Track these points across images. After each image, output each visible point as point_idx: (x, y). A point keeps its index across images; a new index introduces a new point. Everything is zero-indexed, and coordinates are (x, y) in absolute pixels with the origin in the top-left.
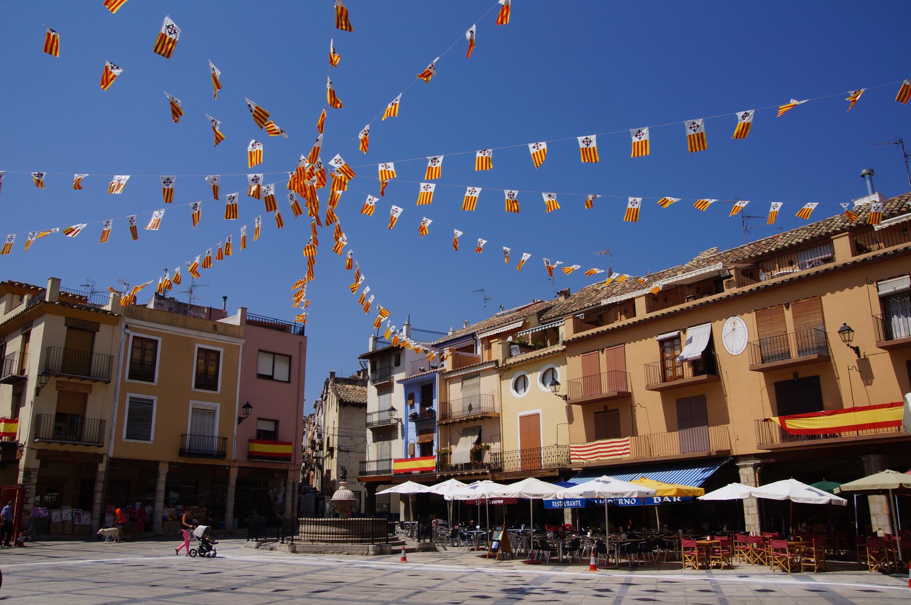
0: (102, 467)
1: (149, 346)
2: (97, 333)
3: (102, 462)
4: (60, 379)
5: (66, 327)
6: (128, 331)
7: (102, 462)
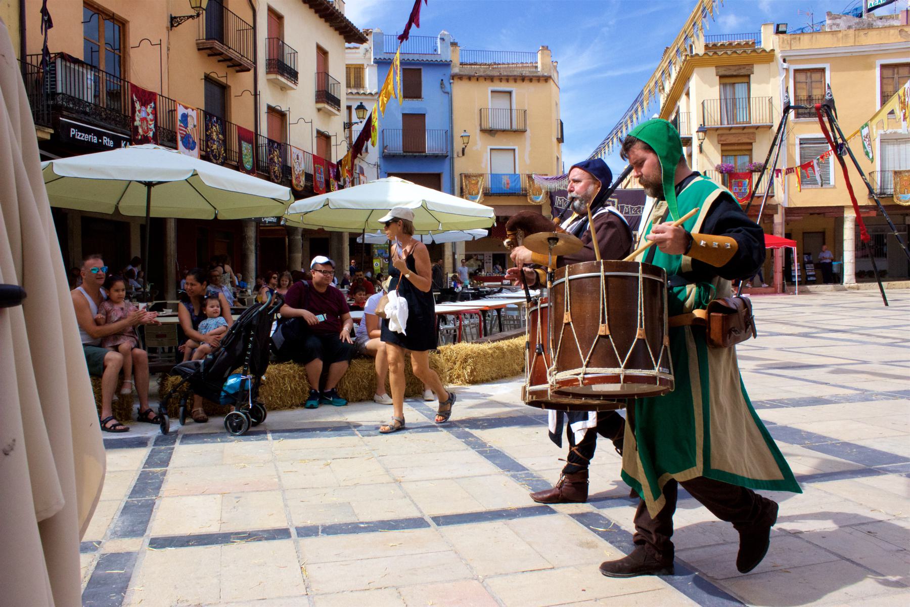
0: (778, 219)
1: (816, 76)
2: (752, 75)
3: (777, 213)
4: (719, 132)
5: (718, 77)
6: (785, 65)
7: (777, 213)
